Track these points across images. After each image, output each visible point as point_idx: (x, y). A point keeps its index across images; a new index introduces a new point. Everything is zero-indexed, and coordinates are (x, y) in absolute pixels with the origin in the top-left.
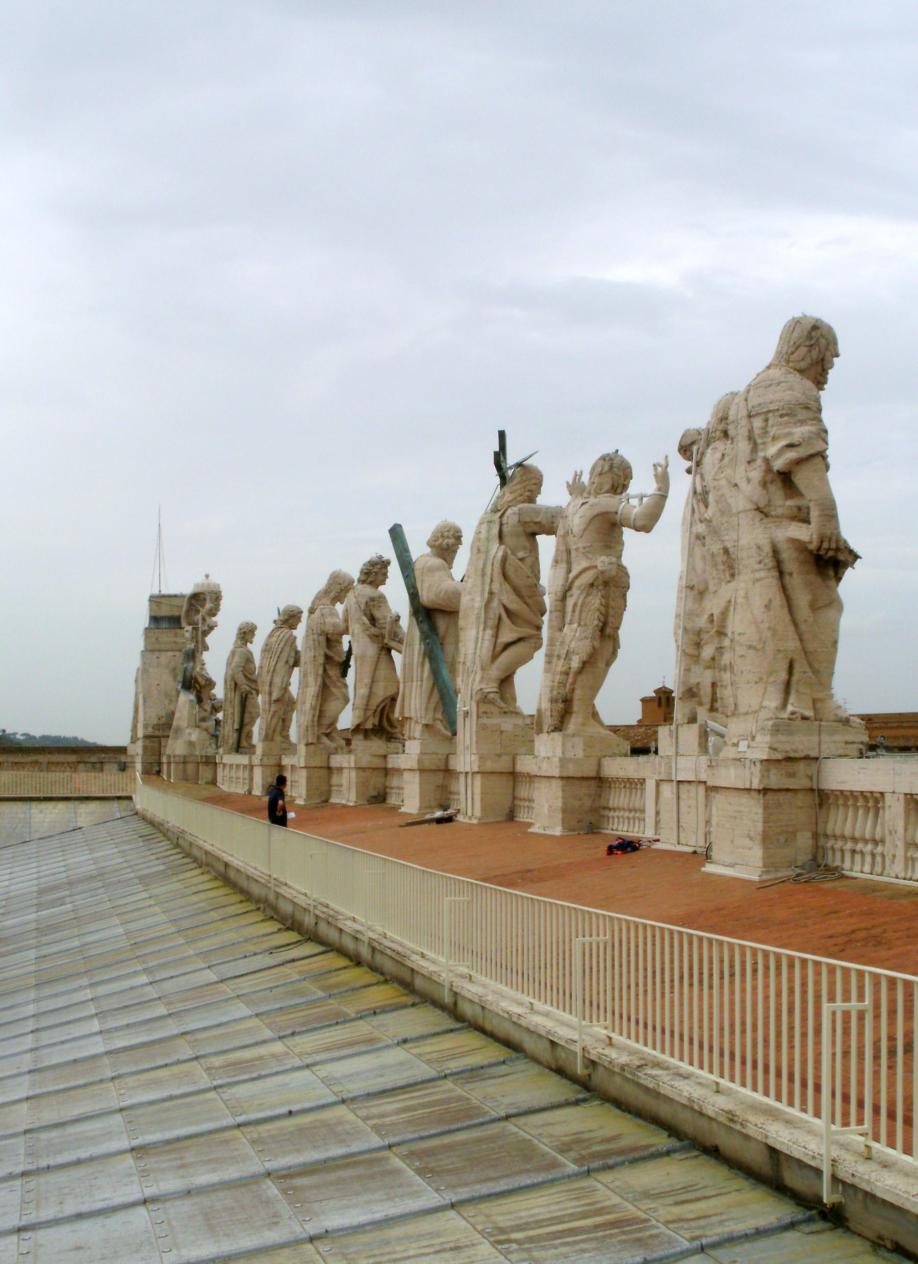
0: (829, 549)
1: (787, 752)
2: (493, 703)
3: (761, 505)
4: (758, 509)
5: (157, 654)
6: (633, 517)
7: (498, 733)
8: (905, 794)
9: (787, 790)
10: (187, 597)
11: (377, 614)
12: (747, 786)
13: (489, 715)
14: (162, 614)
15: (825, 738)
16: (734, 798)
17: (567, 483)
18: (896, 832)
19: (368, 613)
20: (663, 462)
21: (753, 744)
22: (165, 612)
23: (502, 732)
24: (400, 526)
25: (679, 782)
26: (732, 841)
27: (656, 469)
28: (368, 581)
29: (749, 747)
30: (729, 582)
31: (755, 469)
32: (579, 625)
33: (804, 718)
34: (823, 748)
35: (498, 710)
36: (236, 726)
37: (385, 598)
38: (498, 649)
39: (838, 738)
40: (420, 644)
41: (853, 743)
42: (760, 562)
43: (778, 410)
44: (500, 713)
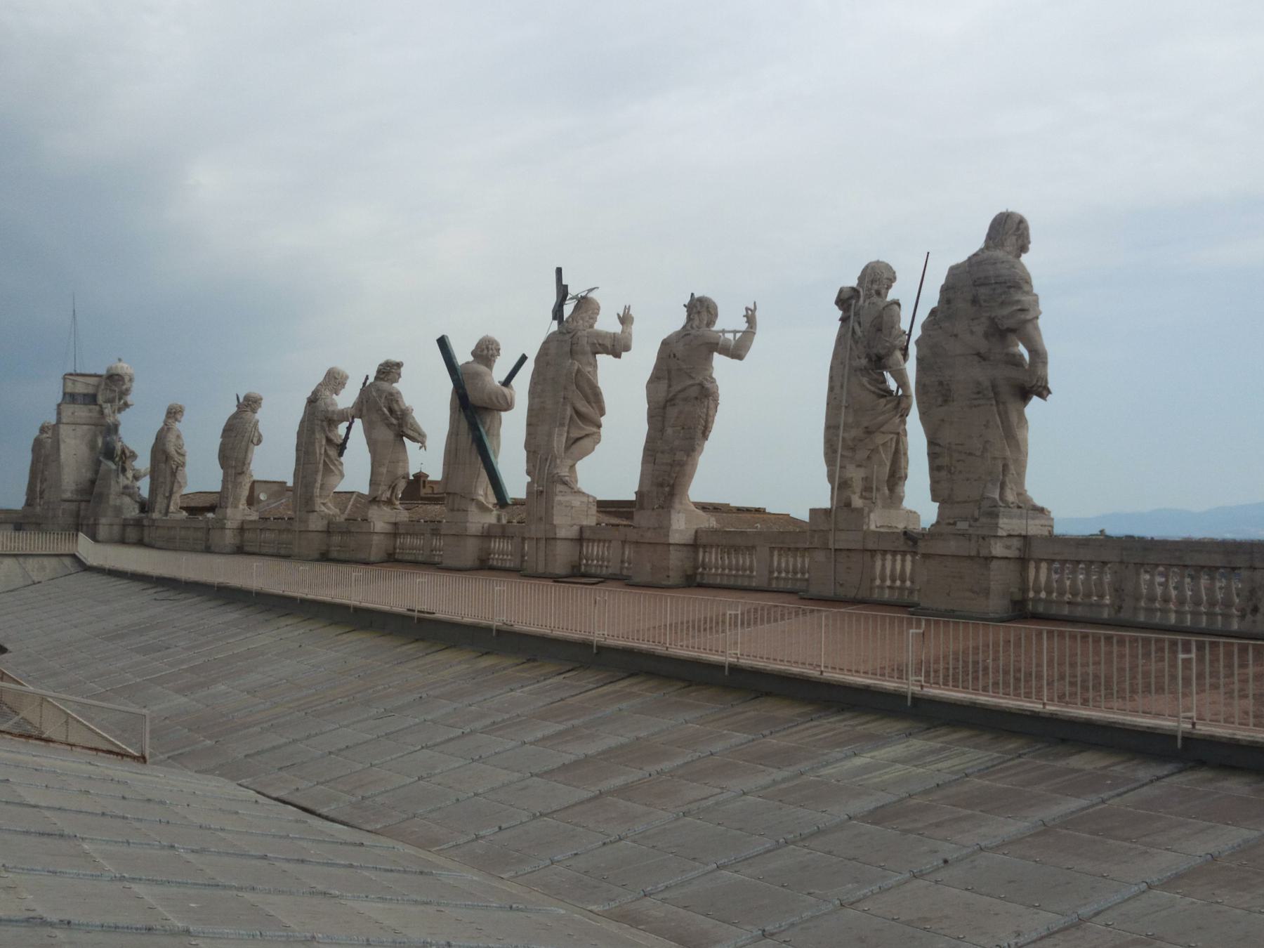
0: (1040, 386)
1: (1009, 531)
2: (566, 484)
3: (982, 351)
4: (978, 354)
5: (73, 427)
6: (732, 347)
7: (569, 508)
8: (1135, 564)
9: (1007, 558)
10: (104, 377)
11: (396, 407)
12: (973, 553)
13: (563, 493)
14: (77, 391)
15: (1030, 522)
16: (1002, 563)
17: (618, 315)
18: (1123, 590)
19: (387, 405)
20: (752, 308)
21: (978, 524)
22: (80, 388)
23: (572, 507)
24: (447, 337)
25: (836, 550)
26: (948, 594)
27: (747, 312)
28: (386, 379)
29: (970, 526)
30: (941, 406)
31: (979, 325)
32: (683, 428)
33: (1019, 507)
34: (1029, 528)
35: (570, 490)
36: (167, 494)
37: (400, 394)
38: (572, 441)
39: (1037, 522)
40: (468, 435)
41: (1045, 526)
42: (979, 393)
43: (1005, 283)
44: (571, 492)
